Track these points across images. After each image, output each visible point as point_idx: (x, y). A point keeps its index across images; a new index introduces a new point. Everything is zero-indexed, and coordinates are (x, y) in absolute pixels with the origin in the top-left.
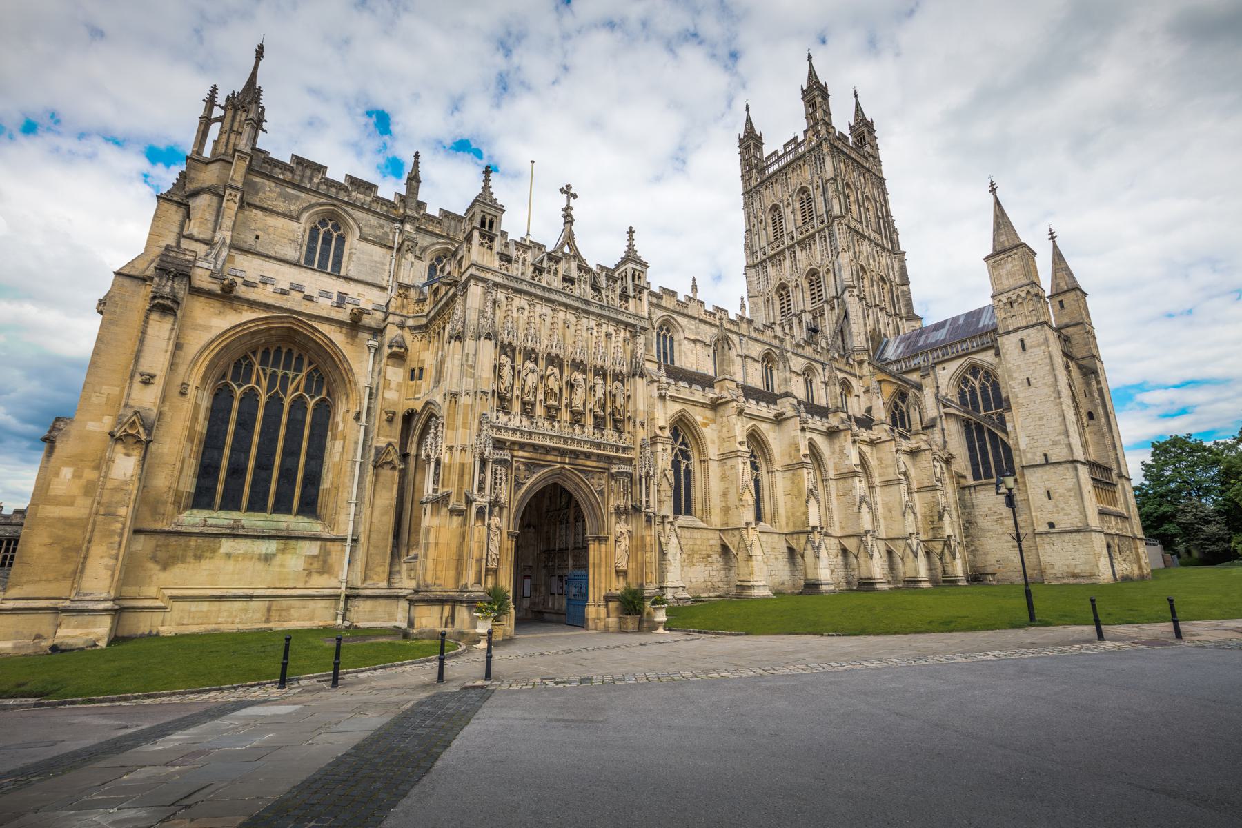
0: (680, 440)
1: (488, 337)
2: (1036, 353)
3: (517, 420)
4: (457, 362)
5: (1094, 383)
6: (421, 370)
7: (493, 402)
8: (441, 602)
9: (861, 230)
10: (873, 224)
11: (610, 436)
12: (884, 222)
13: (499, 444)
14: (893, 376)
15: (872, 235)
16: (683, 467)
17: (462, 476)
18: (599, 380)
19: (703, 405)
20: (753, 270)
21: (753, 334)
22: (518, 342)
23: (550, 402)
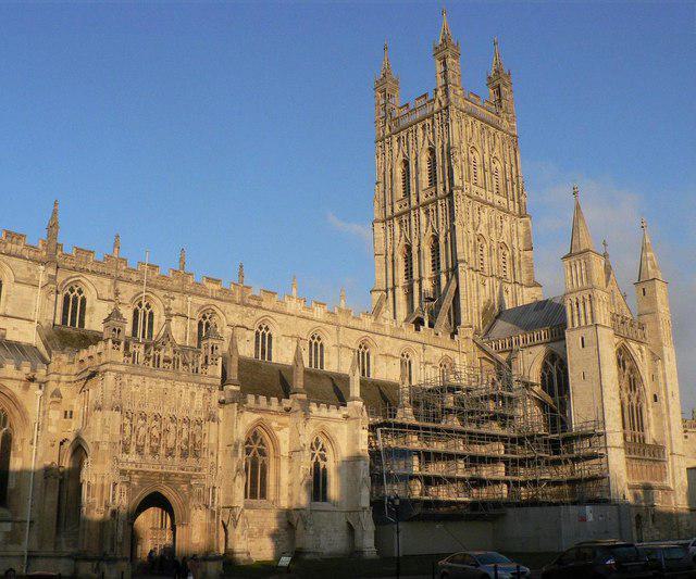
0: (259, 441)
1: (117, 409)
2: (591, 350)
3: (133, 457)
4: (99, 424)
5: (659, 367)
6: (71, 412)
7: (120, 447)
8: (91, 560)
9: (483, 198)
10: (501, 187)
11: (191, 461)
12: (513, 183)
13: (123, 472)
14: (492, 357)
15: (497, 198)
16: (260, 463)
17: (102, 492)
18: (185, 426)
19: (276, 413)
20: (381, 225)
21: (351, 324)
22: (136, 409)
23: (153, 444)
